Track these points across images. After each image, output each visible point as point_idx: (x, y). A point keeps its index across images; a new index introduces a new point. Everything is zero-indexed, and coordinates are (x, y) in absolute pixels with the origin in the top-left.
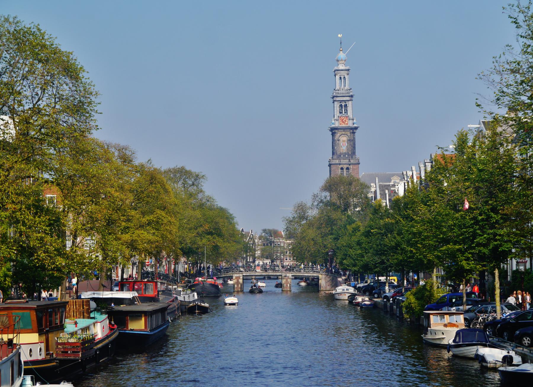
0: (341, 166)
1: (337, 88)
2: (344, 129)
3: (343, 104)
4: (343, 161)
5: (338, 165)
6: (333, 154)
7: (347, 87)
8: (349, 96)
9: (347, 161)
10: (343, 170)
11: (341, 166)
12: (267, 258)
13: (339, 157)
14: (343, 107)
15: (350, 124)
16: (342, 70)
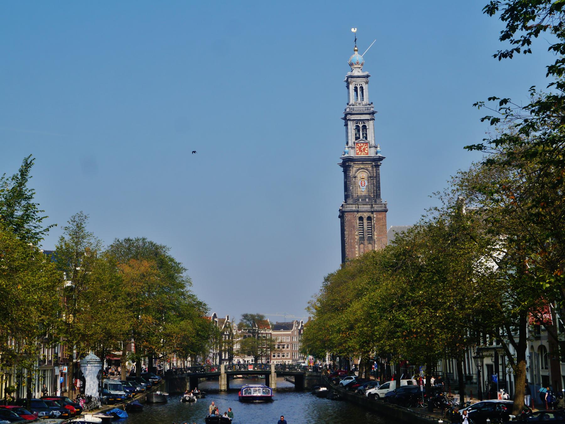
0: (359, 215)
1: (352, 101)
2: (363, 160)
3: (361, 125)
4: (363, 208)
5: (356, 213)
6: (346, 197)
7: (366, 101)
8: (369, 114)
9: (367, 207)
10: (363, 221)
11: (359, 215)
12: (249, 355)
13: (356, 201)
14: (361, 129)
15: (372, 153)
16: (359, 77)
